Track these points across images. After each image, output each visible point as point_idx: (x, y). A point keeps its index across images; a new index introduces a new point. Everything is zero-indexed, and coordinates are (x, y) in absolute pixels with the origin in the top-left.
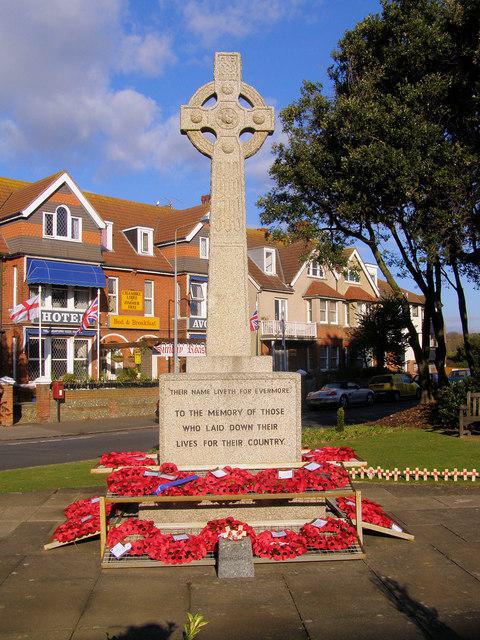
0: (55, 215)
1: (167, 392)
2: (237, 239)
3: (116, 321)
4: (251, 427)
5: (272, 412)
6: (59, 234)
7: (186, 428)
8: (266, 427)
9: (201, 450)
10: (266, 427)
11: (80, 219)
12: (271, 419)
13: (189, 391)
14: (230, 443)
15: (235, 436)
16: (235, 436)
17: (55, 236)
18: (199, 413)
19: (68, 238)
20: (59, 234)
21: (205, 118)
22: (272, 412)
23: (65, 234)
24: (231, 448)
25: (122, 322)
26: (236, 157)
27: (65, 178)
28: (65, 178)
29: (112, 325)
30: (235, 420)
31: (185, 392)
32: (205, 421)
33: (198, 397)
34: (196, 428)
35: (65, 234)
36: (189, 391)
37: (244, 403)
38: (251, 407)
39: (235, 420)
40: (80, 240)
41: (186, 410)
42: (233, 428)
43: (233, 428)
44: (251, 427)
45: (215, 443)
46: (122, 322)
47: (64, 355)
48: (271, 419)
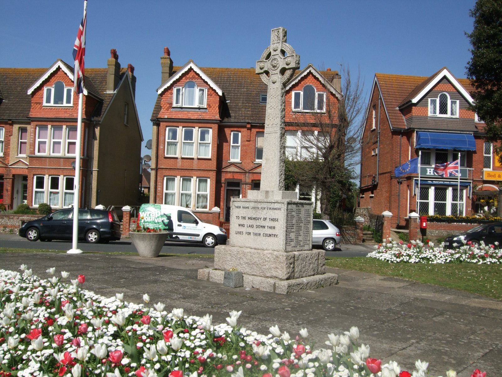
0: (438, 100)
1: (234, 207)
2: (275, 129)
3: (489, 175)
4: (264, 227)
5: (273, 220)
6: (441, 112)
7: (239, 225)
8: (270, 228)
9: (245, 236)
10: (270, 228)
11: (458, 102)
12: (272, 224)
13: (242, 207)
14: (256, 234)
15: (257, 231)
16: (257, 231)
17: (438, 115)
18: (244, 218)
19: (449, 115)
20: (441, 112)
21: (266, 66)
22: (273, 220)
23: (446, 112)
24: (256, 237)
25: (494, 176)
26: (279, 85)
27: (445, 73)
28: (445, 73)
29: (486, 178)
30: (258, 223)
31: (240, 207)
32: (247, 222)
33: (245, 210)
34: (243, 225)
35: (446, 112)
36: (242, 207)
37: (262, 214)
38: (265, 217)
39: (258, 223)
40: (457, 116)
41: (240, 216)
42: (258, 227)
43: (258, 227)
44: (264, 227)
45: (250, 233)
46: (494, 176)
47: (444, 199)
48: (272, 224)
